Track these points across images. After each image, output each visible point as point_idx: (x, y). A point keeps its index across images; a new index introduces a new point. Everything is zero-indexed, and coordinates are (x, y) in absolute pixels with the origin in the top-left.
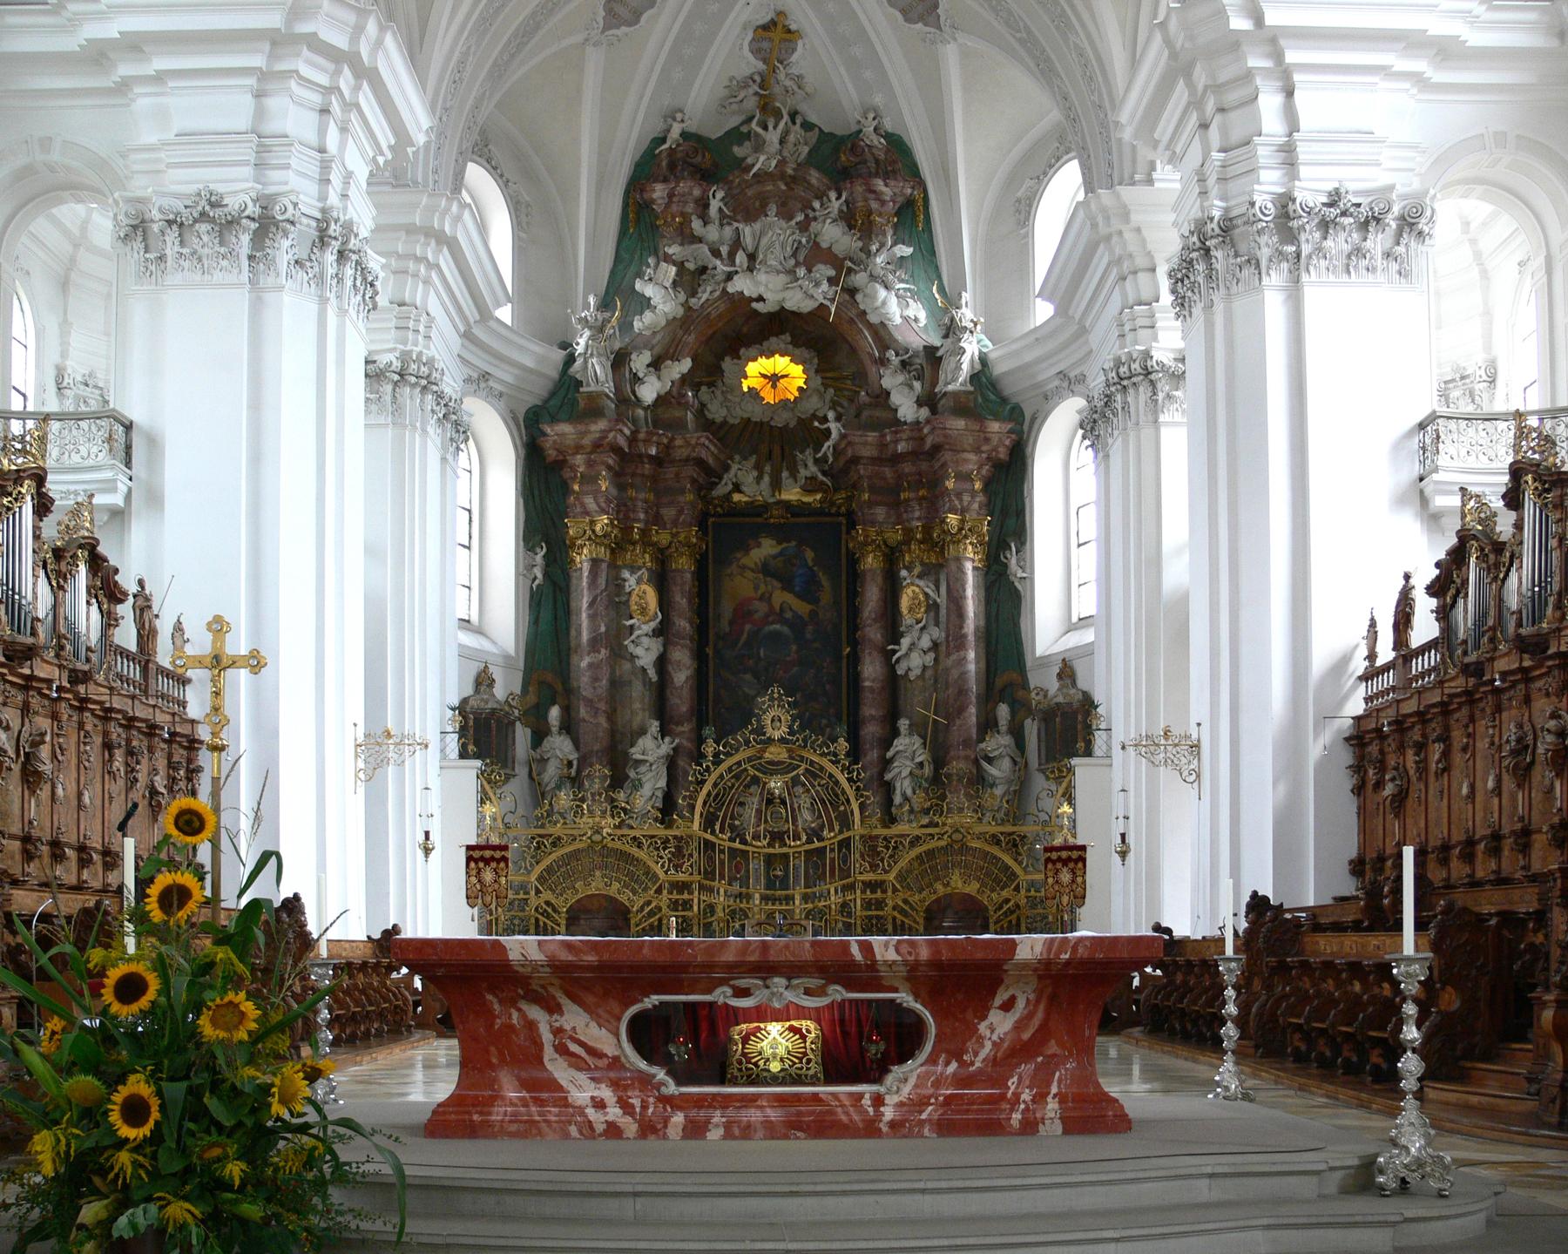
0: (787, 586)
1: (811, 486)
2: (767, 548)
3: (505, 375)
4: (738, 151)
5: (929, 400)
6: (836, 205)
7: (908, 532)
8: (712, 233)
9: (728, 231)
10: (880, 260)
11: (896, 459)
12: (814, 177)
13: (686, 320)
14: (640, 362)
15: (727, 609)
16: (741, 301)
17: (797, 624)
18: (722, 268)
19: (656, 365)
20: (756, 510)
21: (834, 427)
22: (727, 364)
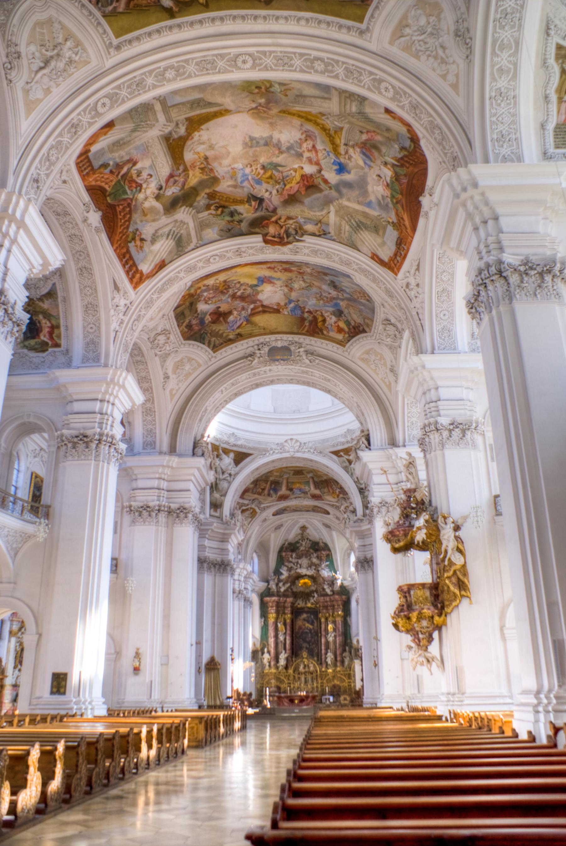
0: (308, 622)
1: (312, 604)
2: (304, 616)
3: (257, 589)
4: (298, 545)
5: (332, 591)
6: (315, 555)
7: (329, 615)
8: (294, 560)
9: (296, 560)
10: (323, 566)
11: (327, 602)
12: (311, 551)
13: (289, 576)
14: (281, 584)
15: (297, 627)
16: (299, 573)
17: (310, 630)
18: (295, 567)
19: (284, 584)
20: (302, 608)
21: (316, 595)
22: (297, 581)
